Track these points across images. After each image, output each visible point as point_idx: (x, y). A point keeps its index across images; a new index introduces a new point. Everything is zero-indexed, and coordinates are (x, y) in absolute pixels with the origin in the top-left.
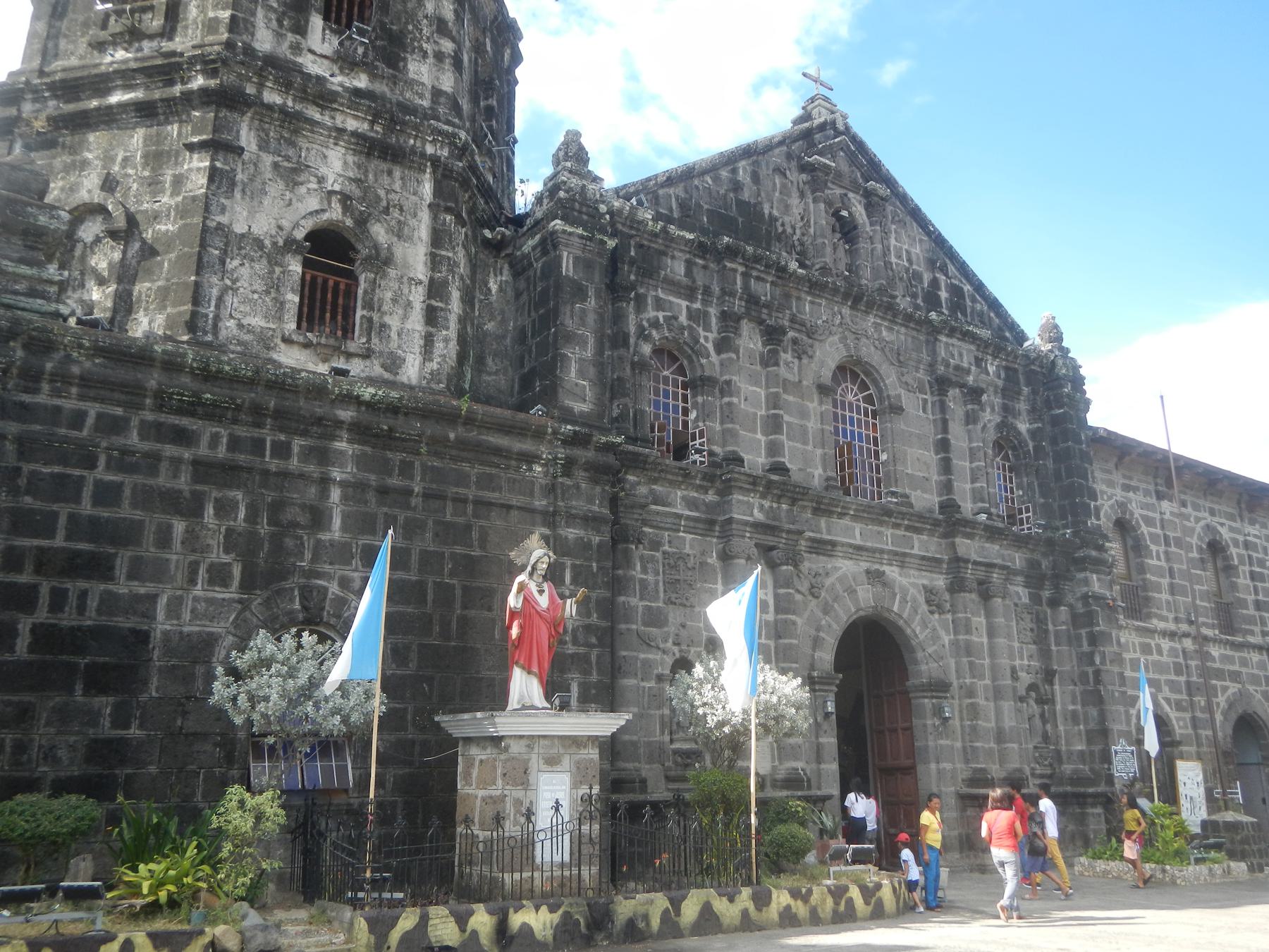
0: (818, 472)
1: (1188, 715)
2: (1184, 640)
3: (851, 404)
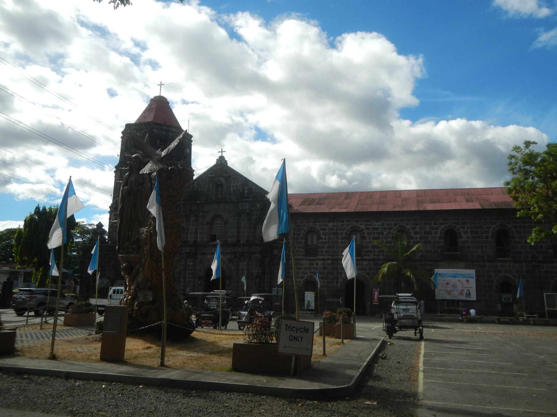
0: (205, 240)
2: (328, 261)
3: (218, 223)
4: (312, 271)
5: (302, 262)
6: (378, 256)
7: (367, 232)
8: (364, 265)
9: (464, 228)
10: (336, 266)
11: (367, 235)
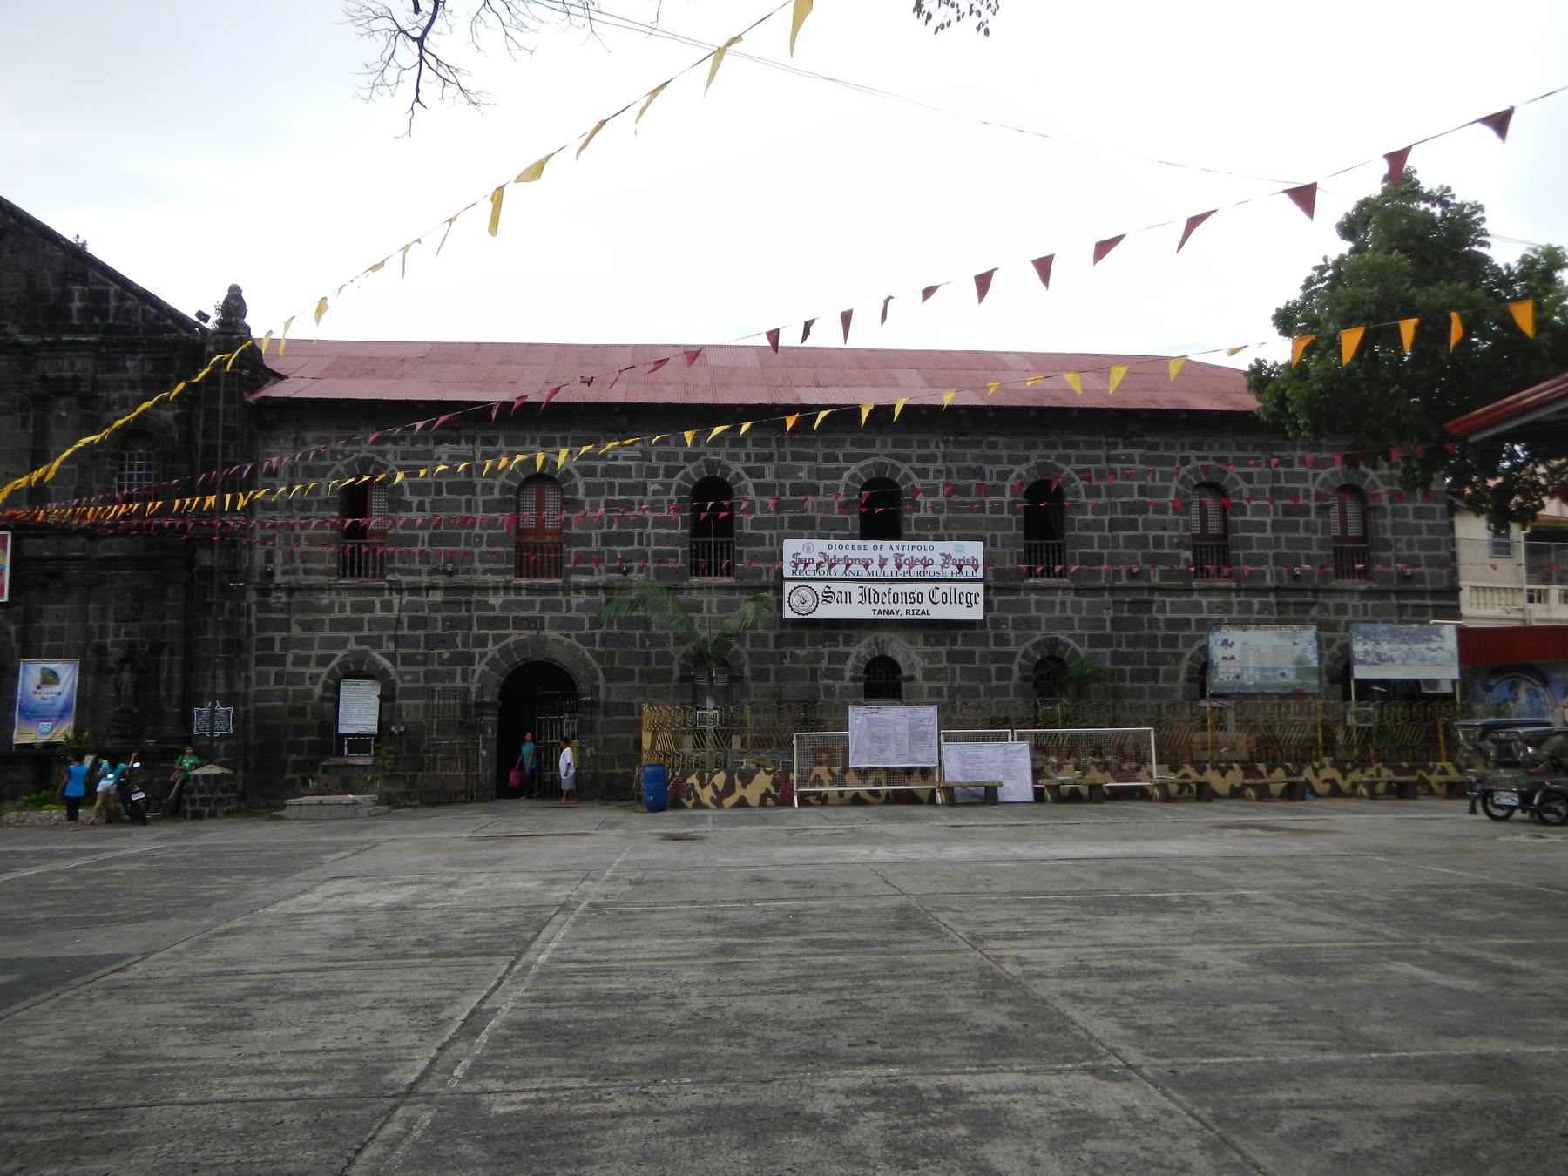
1: (421, 669)
4: (366, 633)
5: (325, 602)
6: (625, 573)
7: (587, 485)
8: (574, 607)
9: (923, 473)
10: (464, 613)
11: (587, 494)
